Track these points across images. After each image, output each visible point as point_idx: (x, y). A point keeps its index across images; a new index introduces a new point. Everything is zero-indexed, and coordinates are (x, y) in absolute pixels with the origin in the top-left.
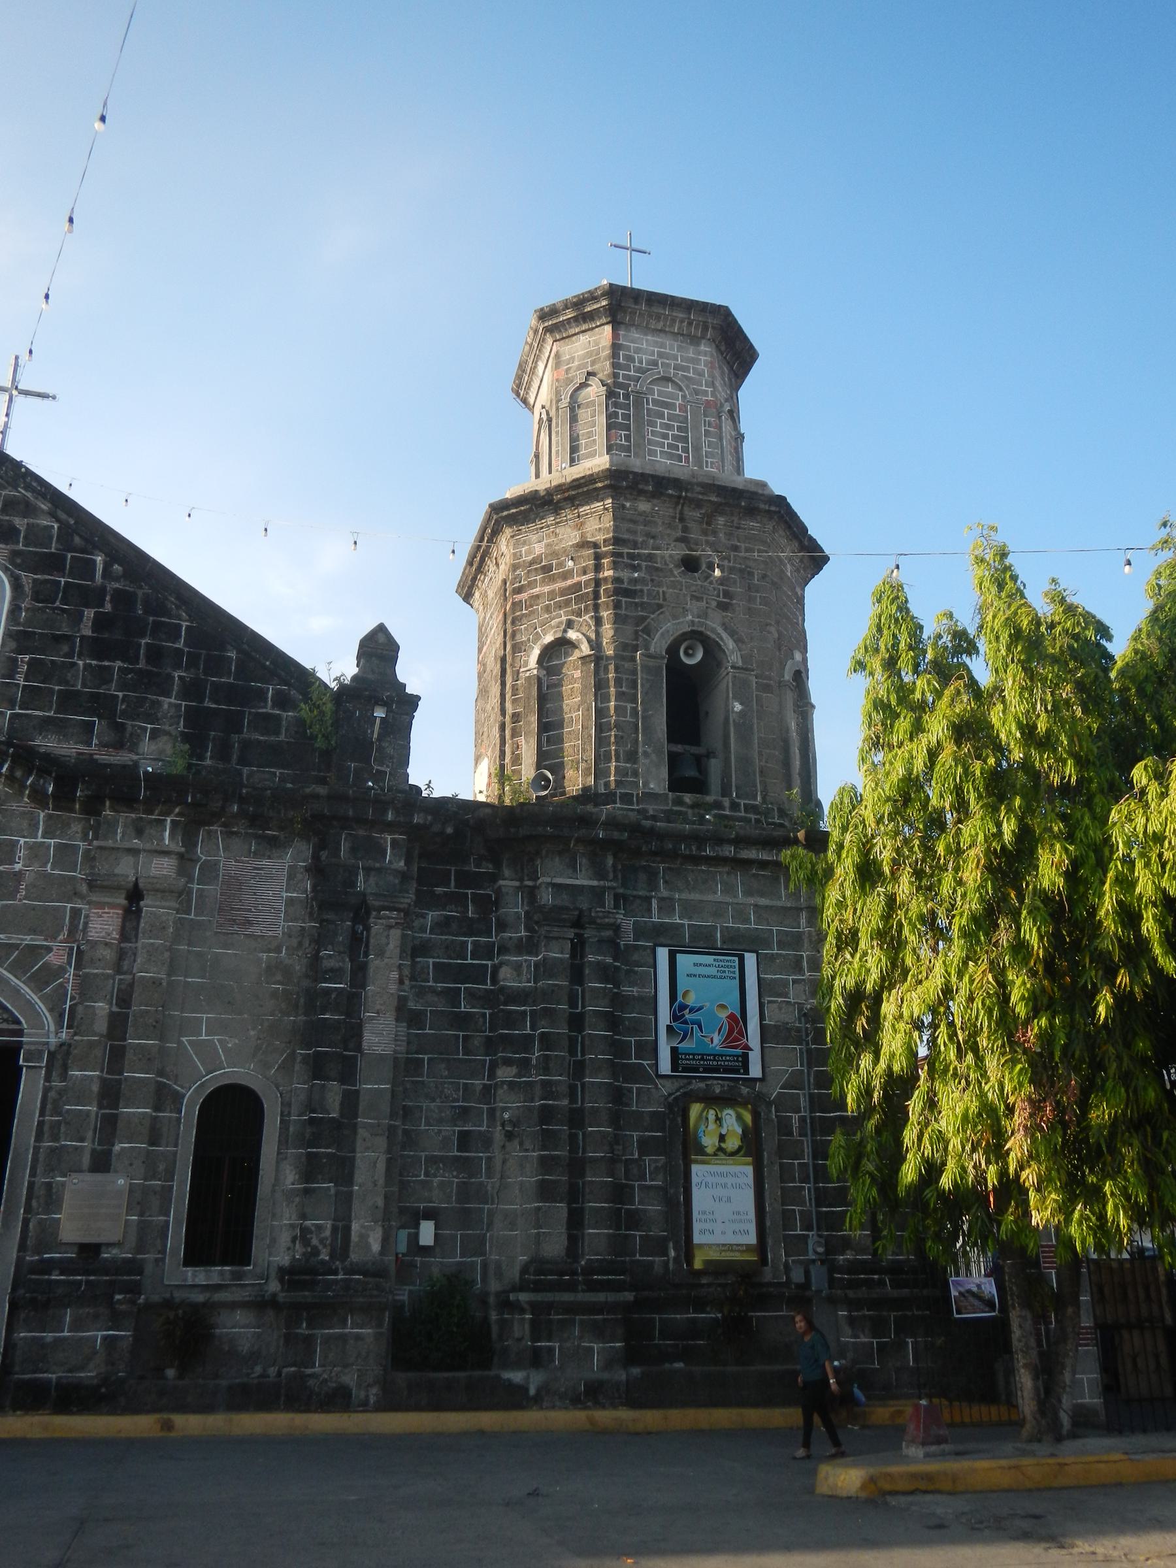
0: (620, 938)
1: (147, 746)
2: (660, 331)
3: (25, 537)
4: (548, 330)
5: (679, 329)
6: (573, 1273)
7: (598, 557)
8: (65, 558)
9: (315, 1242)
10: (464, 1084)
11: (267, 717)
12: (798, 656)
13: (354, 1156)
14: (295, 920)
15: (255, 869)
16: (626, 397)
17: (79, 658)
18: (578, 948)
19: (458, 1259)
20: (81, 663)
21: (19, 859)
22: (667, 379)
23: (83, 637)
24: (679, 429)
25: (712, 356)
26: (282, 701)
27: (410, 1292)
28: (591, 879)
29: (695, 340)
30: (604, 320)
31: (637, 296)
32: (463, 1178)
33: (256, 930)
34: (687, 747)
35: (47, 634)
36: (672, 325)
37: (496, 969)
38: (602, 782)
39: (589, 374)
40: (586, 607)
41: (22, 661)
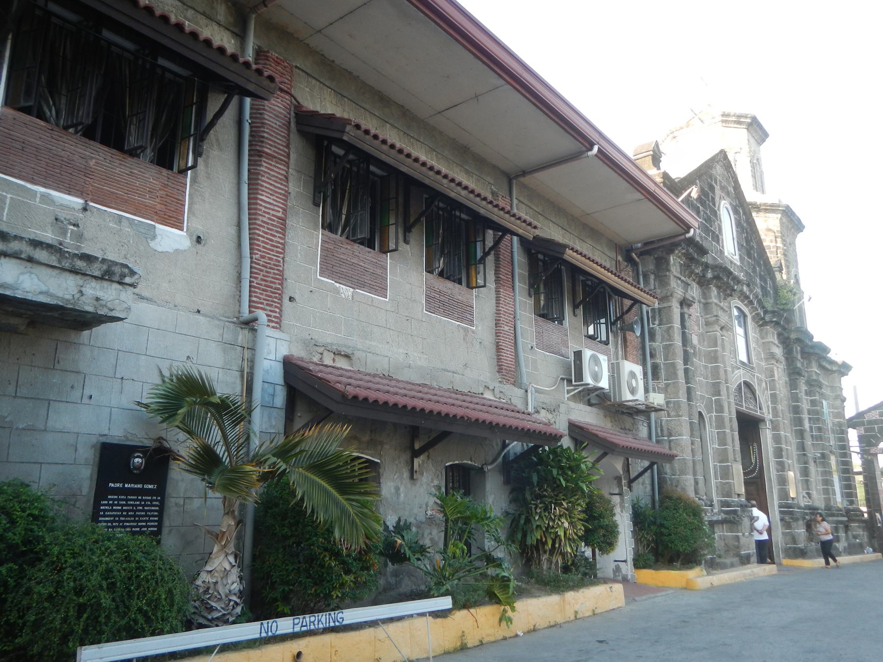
2: (754, 137)
4: (723, 121)
7: (776, 237)
30: (744, 127)
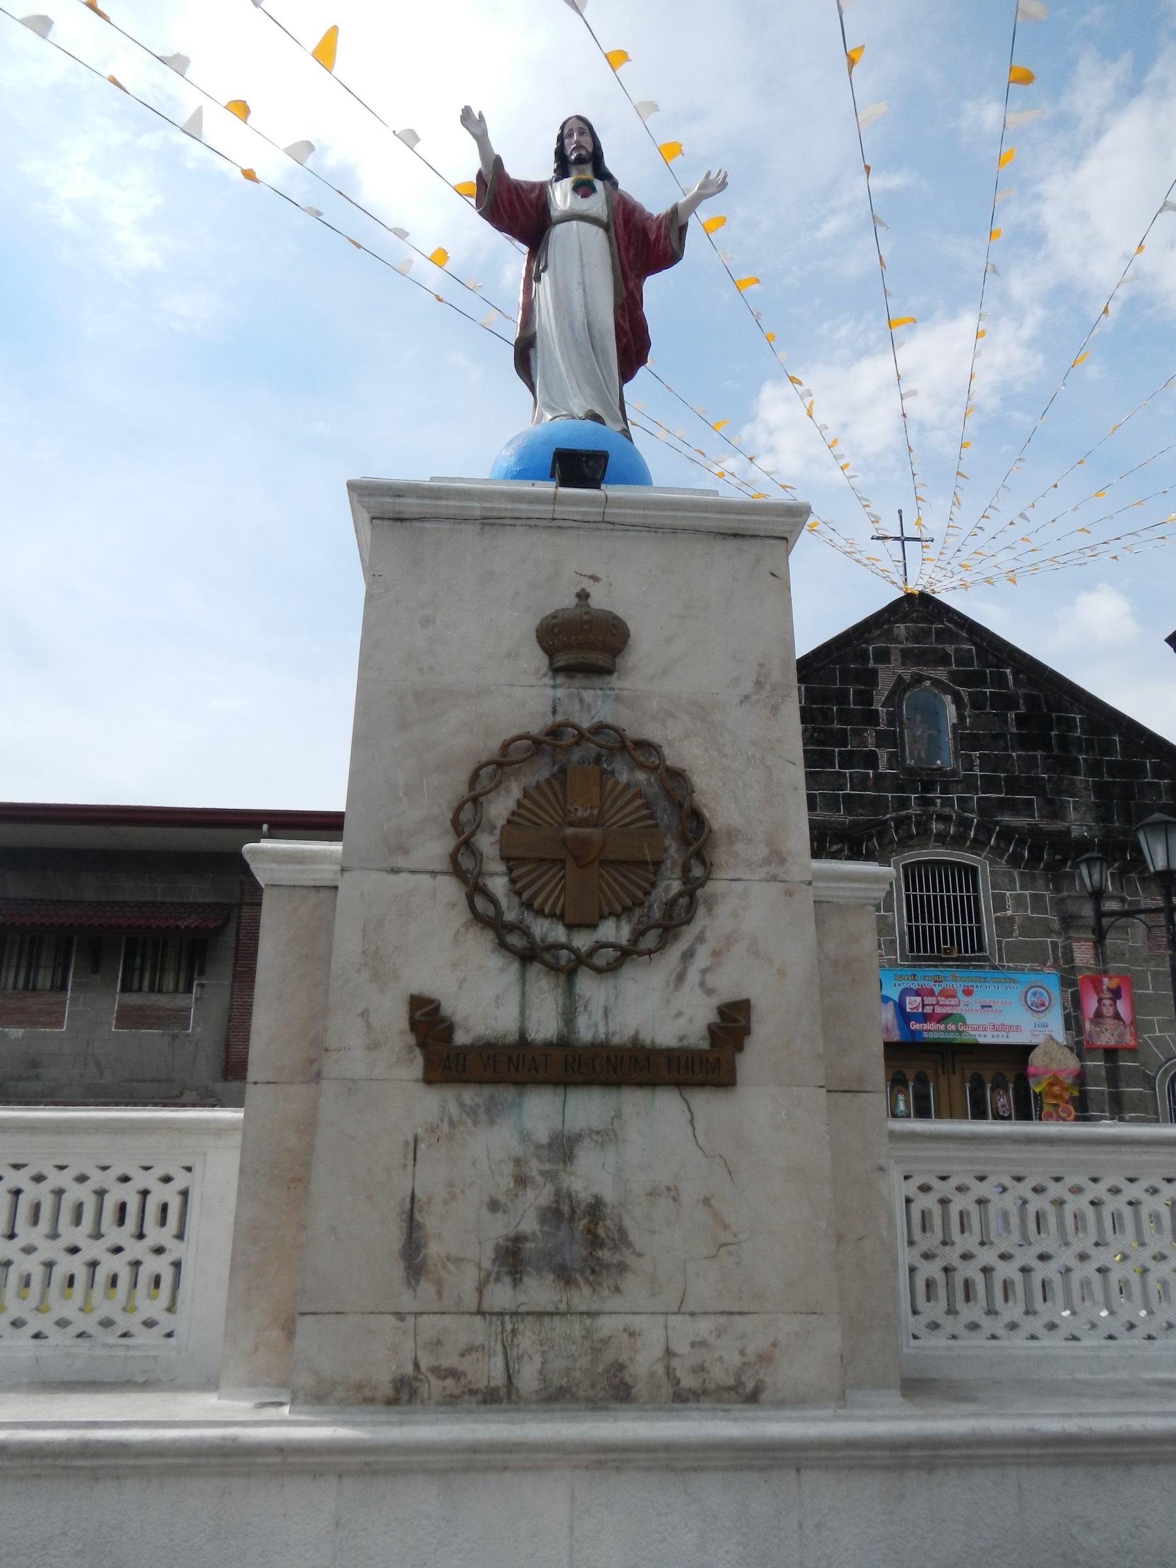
1: (1072, 815)
3: (955, 661)
8: (985, 672)
11: (1150, 784)
17: (1013, 750)
20: (1014, 754)
21: (1009, 907)
23: (1012, 734)
35: (987, 734)
41: (975, 757)
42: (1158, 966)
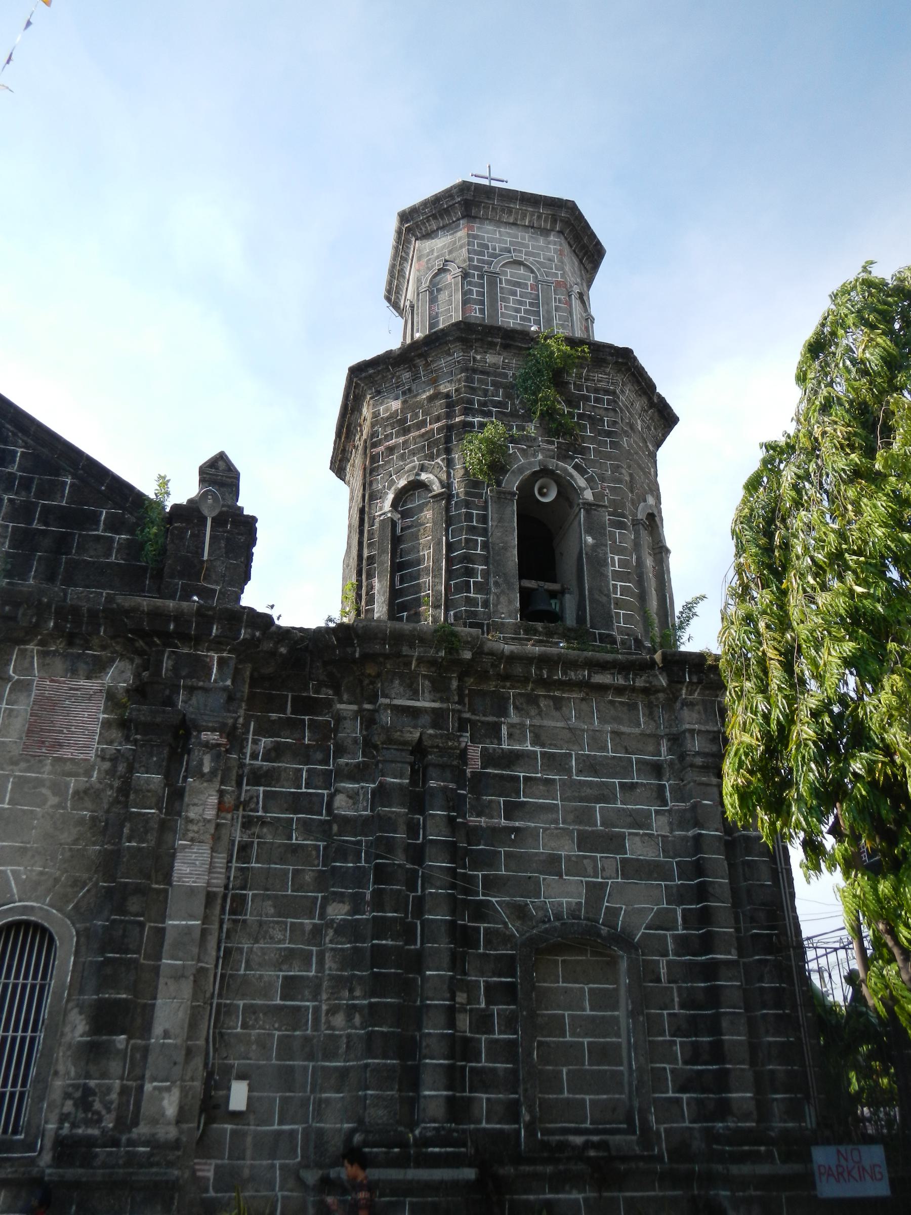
0: (466, 764)
2: (514, 224)
5: (529, 222)
6: (404, 1145)
7: (450, 405)
9: (97, 1106)
10: (292, 923)
11: (98, 537)
12: (651, 500)
13: (153, 1005)
14: (111, 743)
15: (71, 689)
16: (481, 277)
18: (419, 774)
19: (276, 1127)
22: (520, 263)
24: (531, 304)
25: (561, 245)
26: (114, 525)
27: (217, 1167)
28: (434, 701)
29: (545, 232)
31: (488, 191)
32: (286, 1030)
33: (66, 753)
34: (541, 583)
36: (523, 218)
37: (332, 797)
38: (452, 613)
39: (446, 261)
40: (437, 451)
42: (28, 770)
